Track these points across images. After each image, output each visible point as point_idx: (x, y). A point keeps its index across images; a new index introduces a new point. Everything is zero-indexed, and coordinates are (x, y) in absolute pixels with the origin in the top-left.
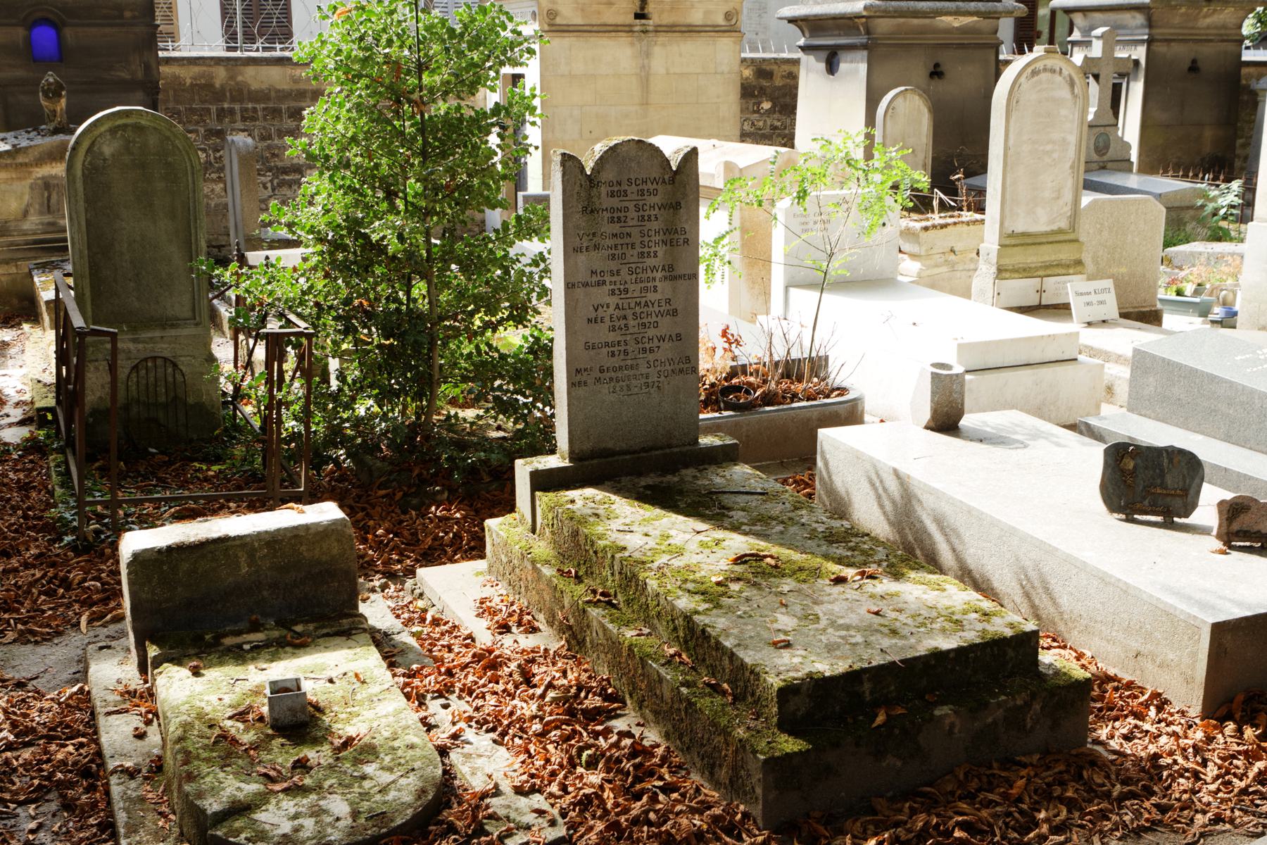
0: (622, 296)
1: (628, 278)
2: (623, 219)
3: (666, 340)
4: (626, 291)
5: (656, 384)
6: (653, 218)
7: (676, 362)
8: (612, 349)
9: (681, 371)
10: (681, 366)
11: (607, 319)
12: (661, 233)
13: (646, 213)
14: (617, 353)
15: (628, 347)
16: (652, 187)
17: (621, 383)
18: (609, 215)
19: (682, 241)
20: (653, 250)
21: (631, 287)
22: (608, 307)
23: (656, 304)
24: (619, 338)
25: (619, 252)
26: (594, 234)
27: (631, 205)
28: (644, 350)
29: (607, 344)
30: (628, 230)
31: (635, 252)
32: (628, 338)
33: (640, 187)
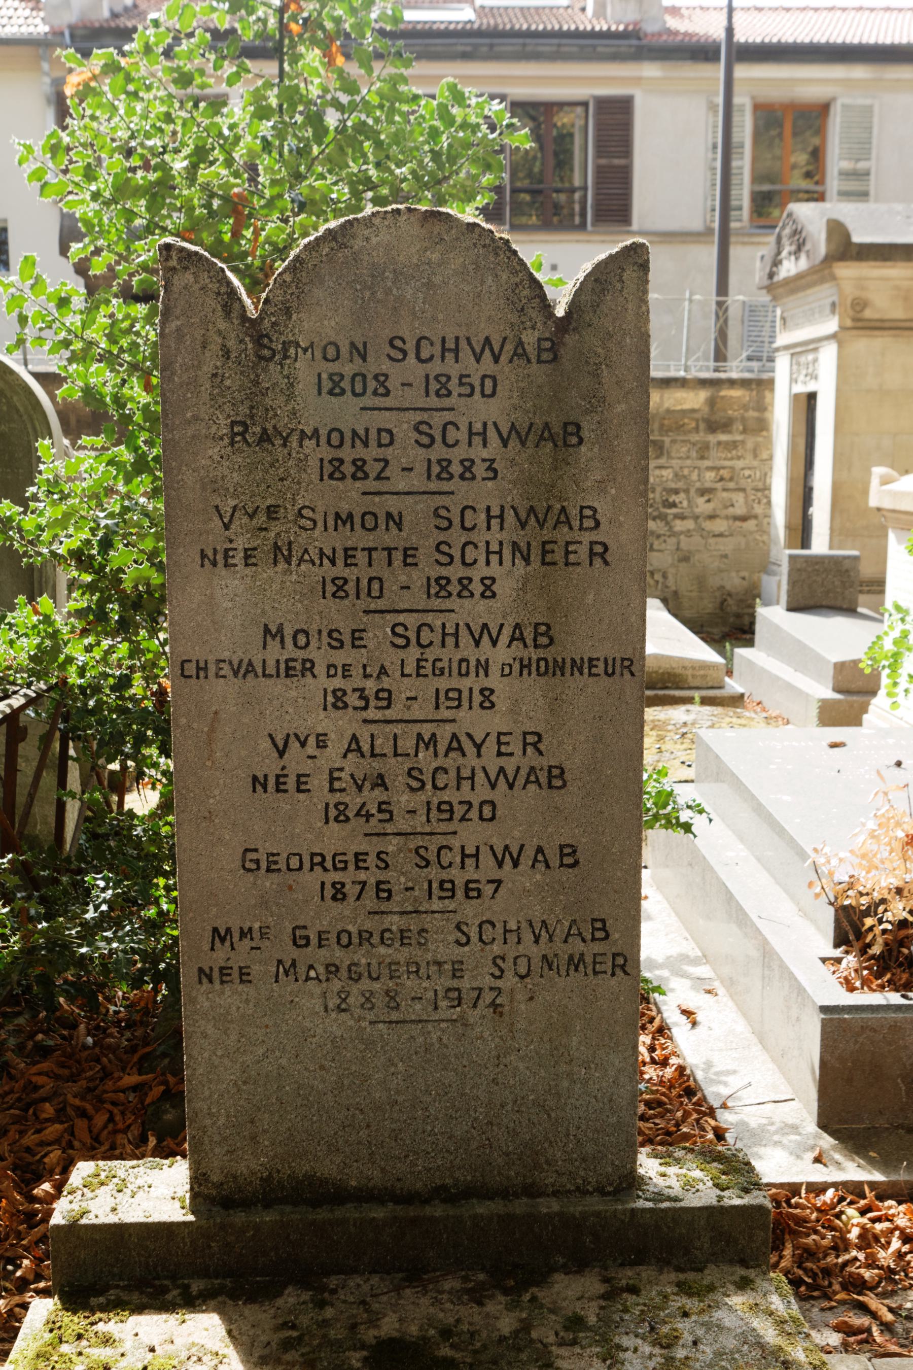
0: (371, 714)
1: (391, 659)
2: (373, 469)
3: (526, 861)
4: (386, 698)
5: (488, 997)
6: (480, 470)
7: (559, 934)
8: (338, 877)
9: (576, 963)
10: (577, 946)
11: (319, 782)
12: (510, 515)
13: (460, 453)
14: (352, 890)
15: (389, 875)
16: (476, 371)
17: (365, 984)
18: (326, 453)
19: (583, 551)
20: (476, 574)
21: (403, 688)
22: (321, 744)
23: (490, 747)
24: (371, 847)
25: (360, 572)
26: (272, 512)
27: (402, 426)
28: (448, 889)
29: (318, 861)
30: (393, 504)
31: (417, 578)
32: (392, 845)
33: (436, 367)
